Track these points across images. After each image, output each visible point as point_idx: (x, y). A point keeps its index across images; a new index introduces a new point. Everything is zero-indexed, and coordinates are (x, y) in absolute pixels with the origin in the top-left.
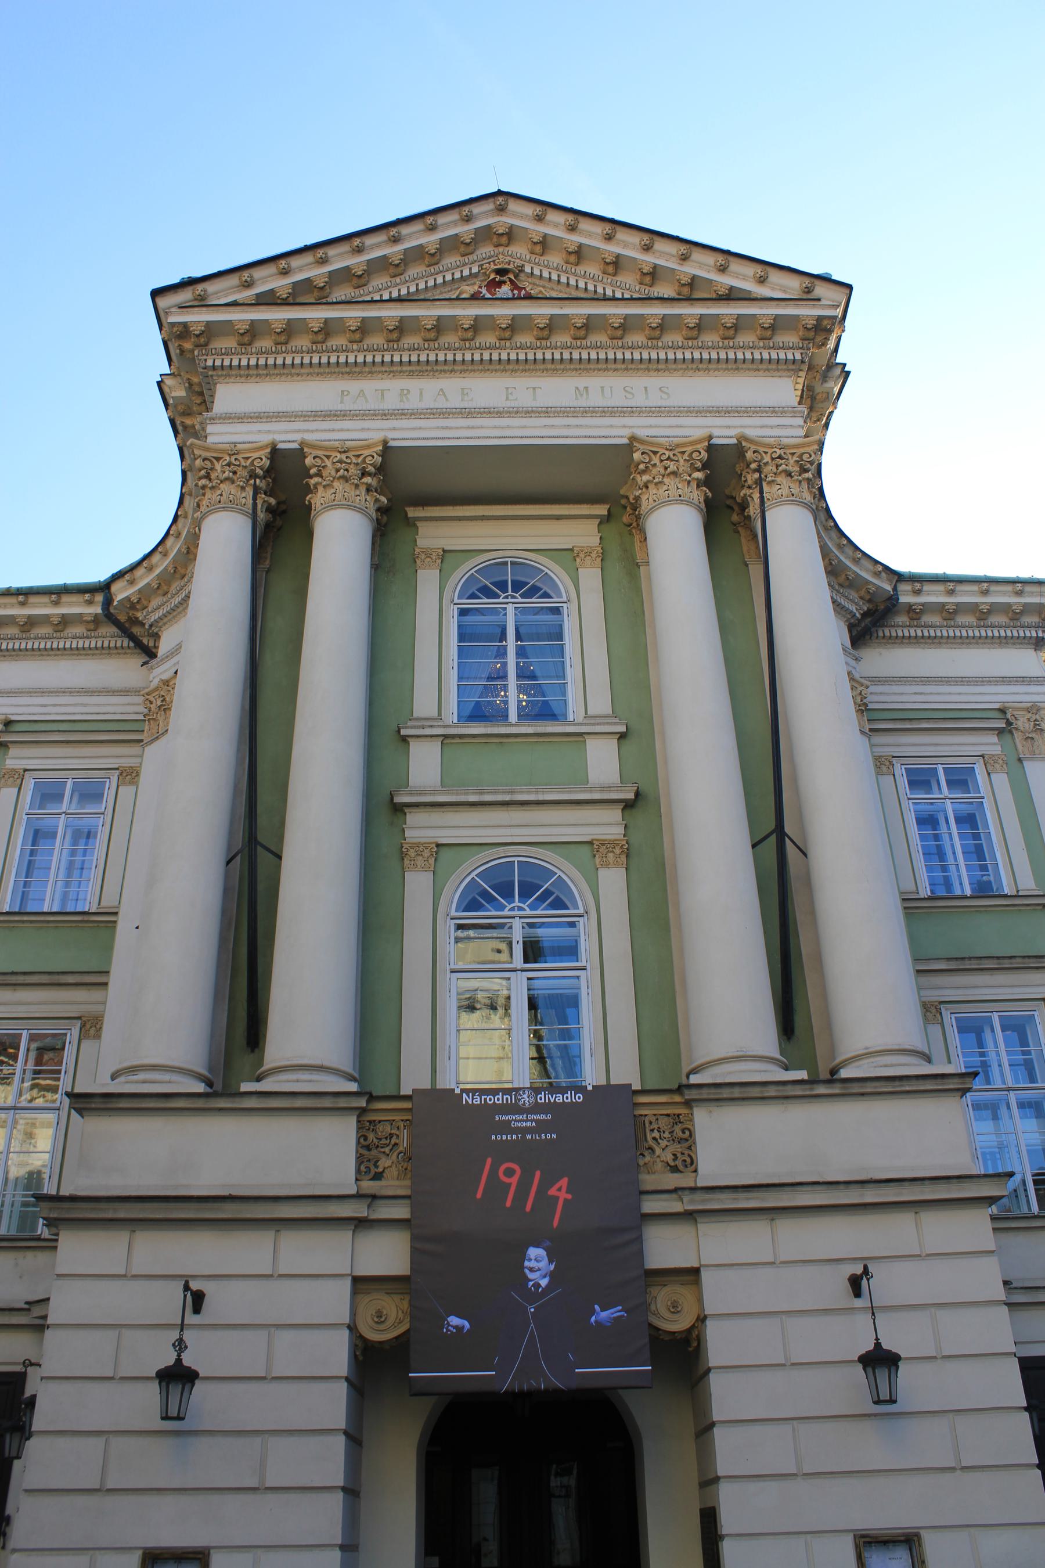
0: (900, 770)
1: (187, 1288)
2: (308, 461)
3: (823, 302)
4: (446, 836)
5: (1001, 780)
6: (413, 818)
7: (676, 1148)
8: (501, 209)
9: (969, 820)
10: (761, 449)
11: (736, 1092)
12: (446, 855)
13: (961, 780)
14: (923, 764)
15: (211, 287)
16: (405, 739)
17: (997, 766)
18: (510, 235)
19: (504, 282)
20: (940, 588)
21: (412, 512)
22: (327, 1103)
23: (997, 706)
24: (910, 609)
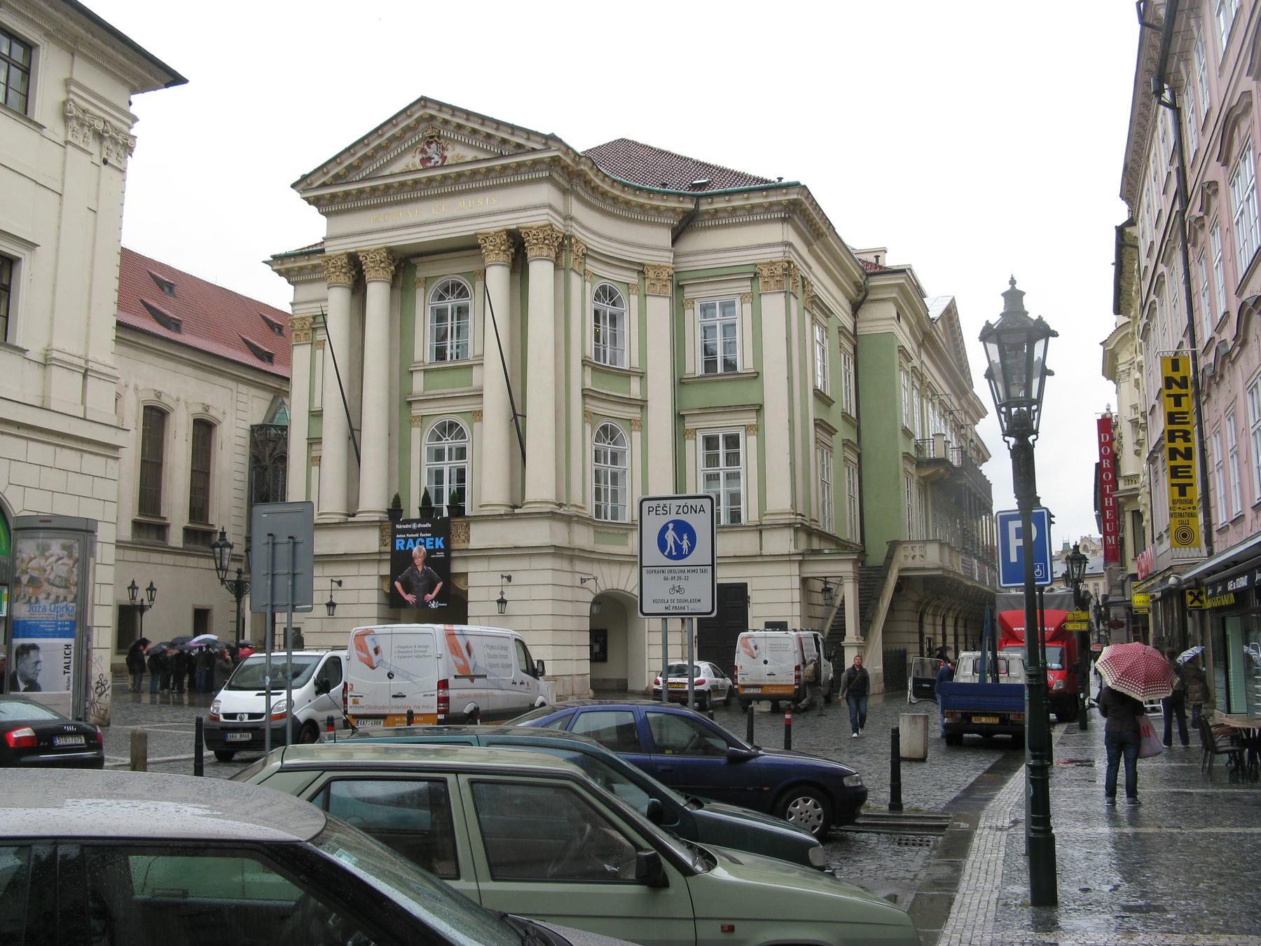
0: (697, 306)
1: (332, 581)
2: (360, 258)
3: (553, 148)
4: (424, 412)
5: (747, 307)
6: (414, 406)
7: (466, 535)
8: (425, 107)
9: (729, 329)
10: (527, 231)
11: (481, 518)
12: (425, 419)
13: (727, 307)
14: (710, 301)
15: (313, 178)
16: (412, 372)
17: (747, 299)
18: (432, 117)
19: (432, 143)
20: (722, 199)
21: (413, 261)
22: (369, 524)
23: (752, 262)
24: (707, 212)
